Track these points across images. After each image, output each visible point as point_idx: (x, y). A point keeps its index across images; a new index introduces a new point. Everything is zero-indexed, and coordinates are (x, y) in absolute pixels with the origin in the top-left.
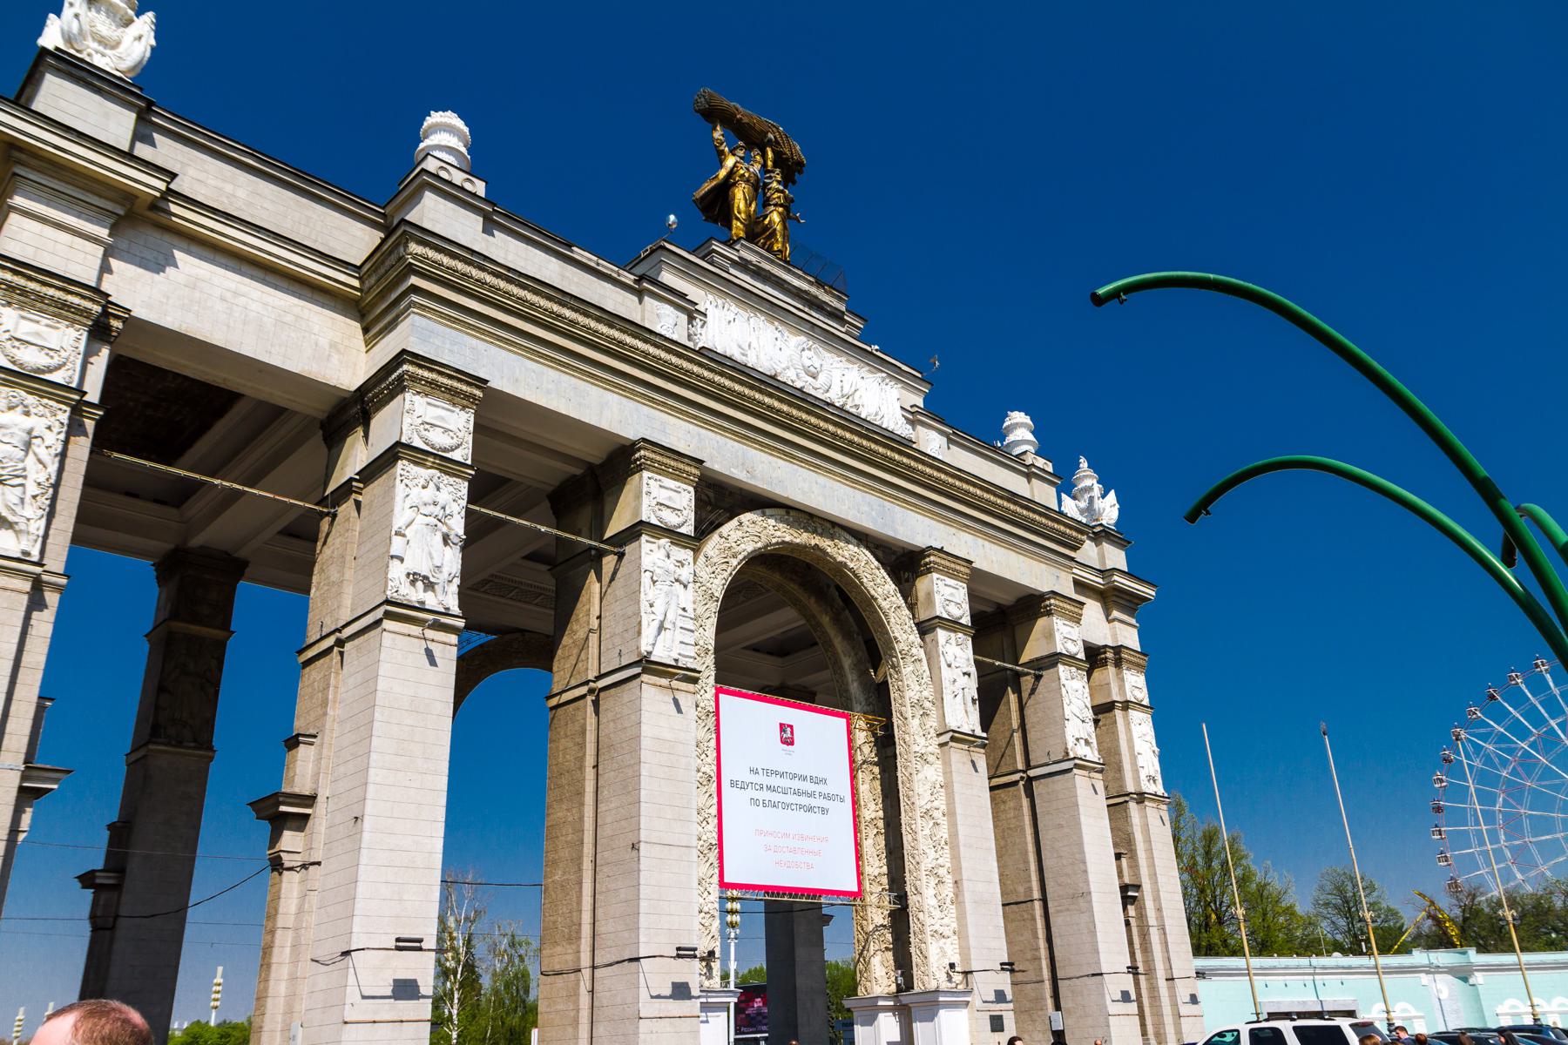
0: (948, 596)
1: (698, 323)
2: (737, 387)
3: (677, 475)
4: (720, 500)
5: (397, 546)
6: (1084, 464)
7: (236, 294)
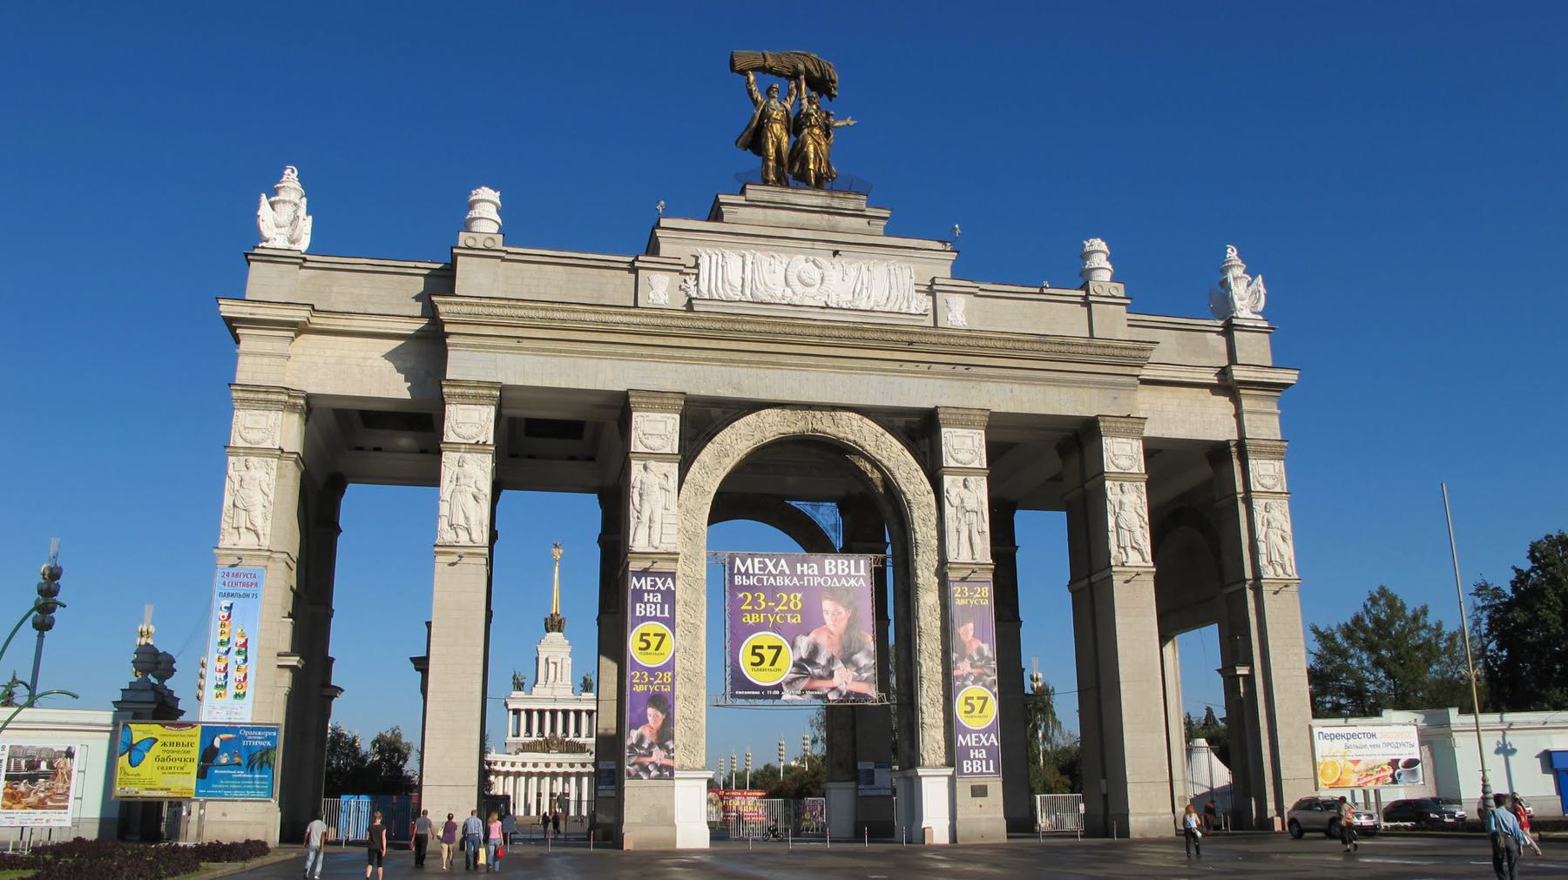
0: (964, 447)
2: (718, 325)
3: (664, 408)
6: (1232, 253)
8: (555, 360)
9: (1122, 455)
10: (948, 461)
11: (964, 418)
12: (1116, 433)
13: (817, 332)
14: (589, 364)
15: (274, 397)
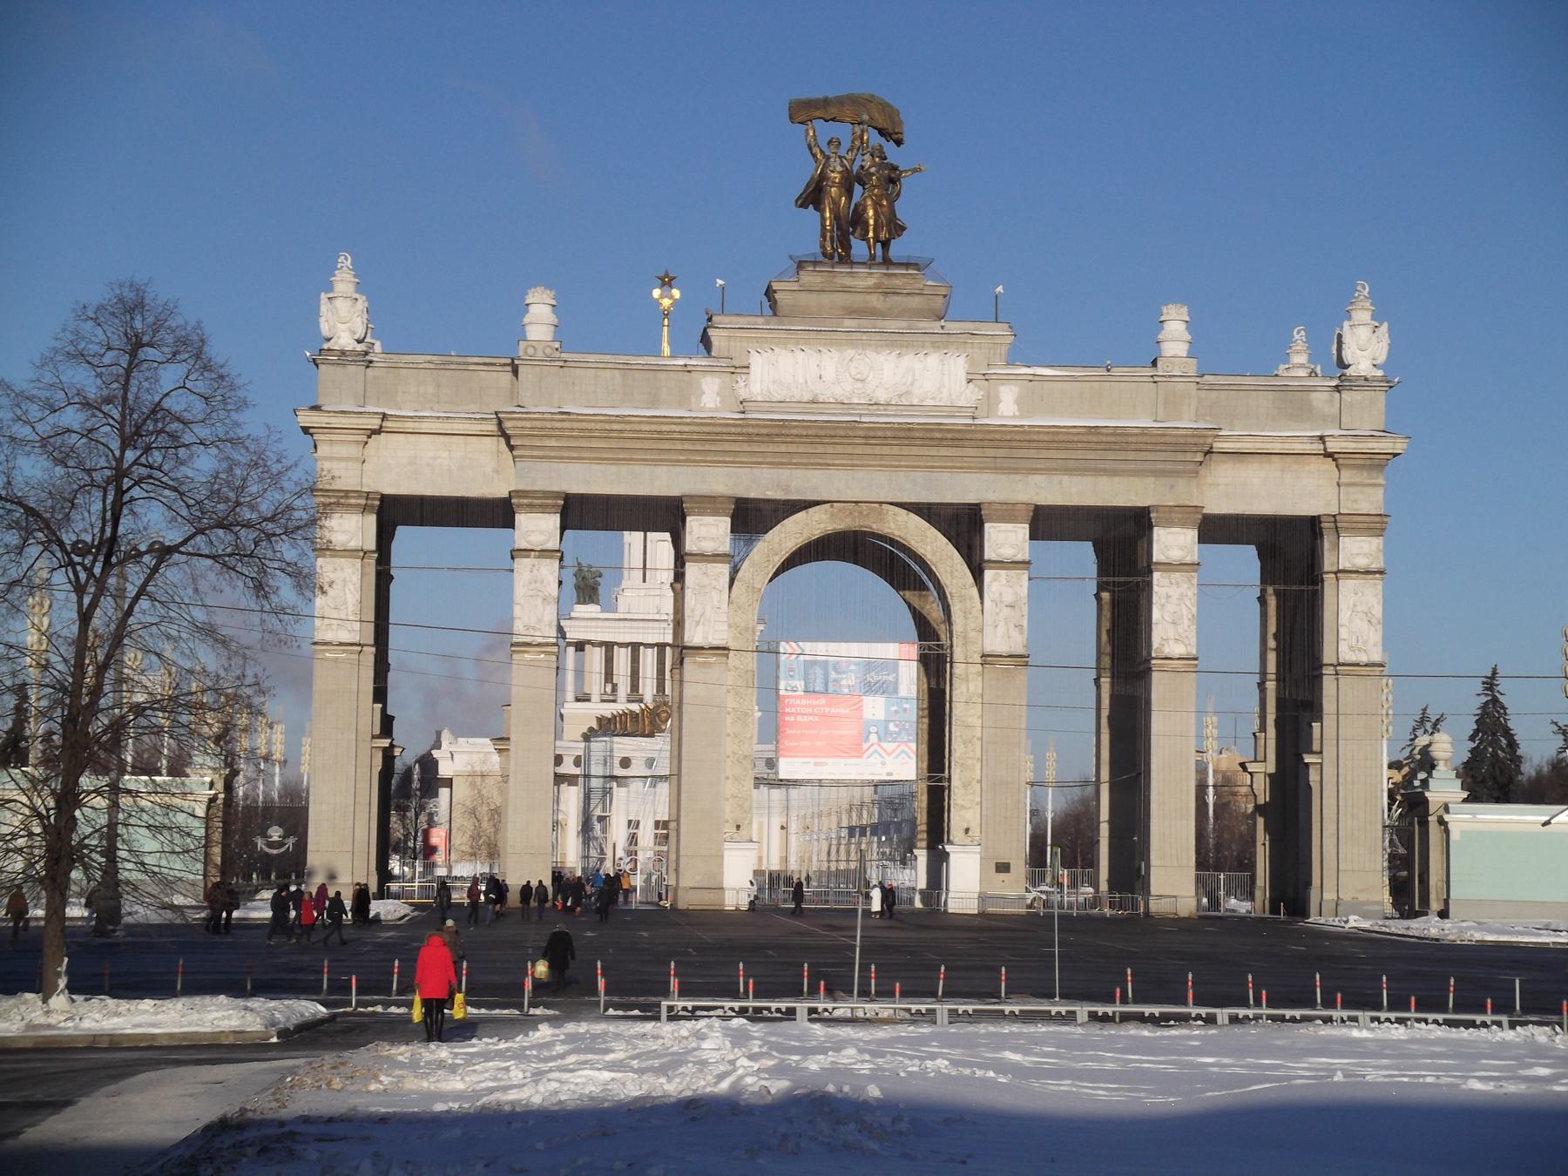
1: (741, 380)
2: (765, 431)
3: (715, 513)
4: (751, 518)
5: (517, 611)
7: (435, 458)
8: (614, 468)
9: (1172, 543)
10: (989, 554)
11: (1008, 513)
12: (1169, 523)
13: (862, 433)
14: (645, 471)
15: (353, 501)
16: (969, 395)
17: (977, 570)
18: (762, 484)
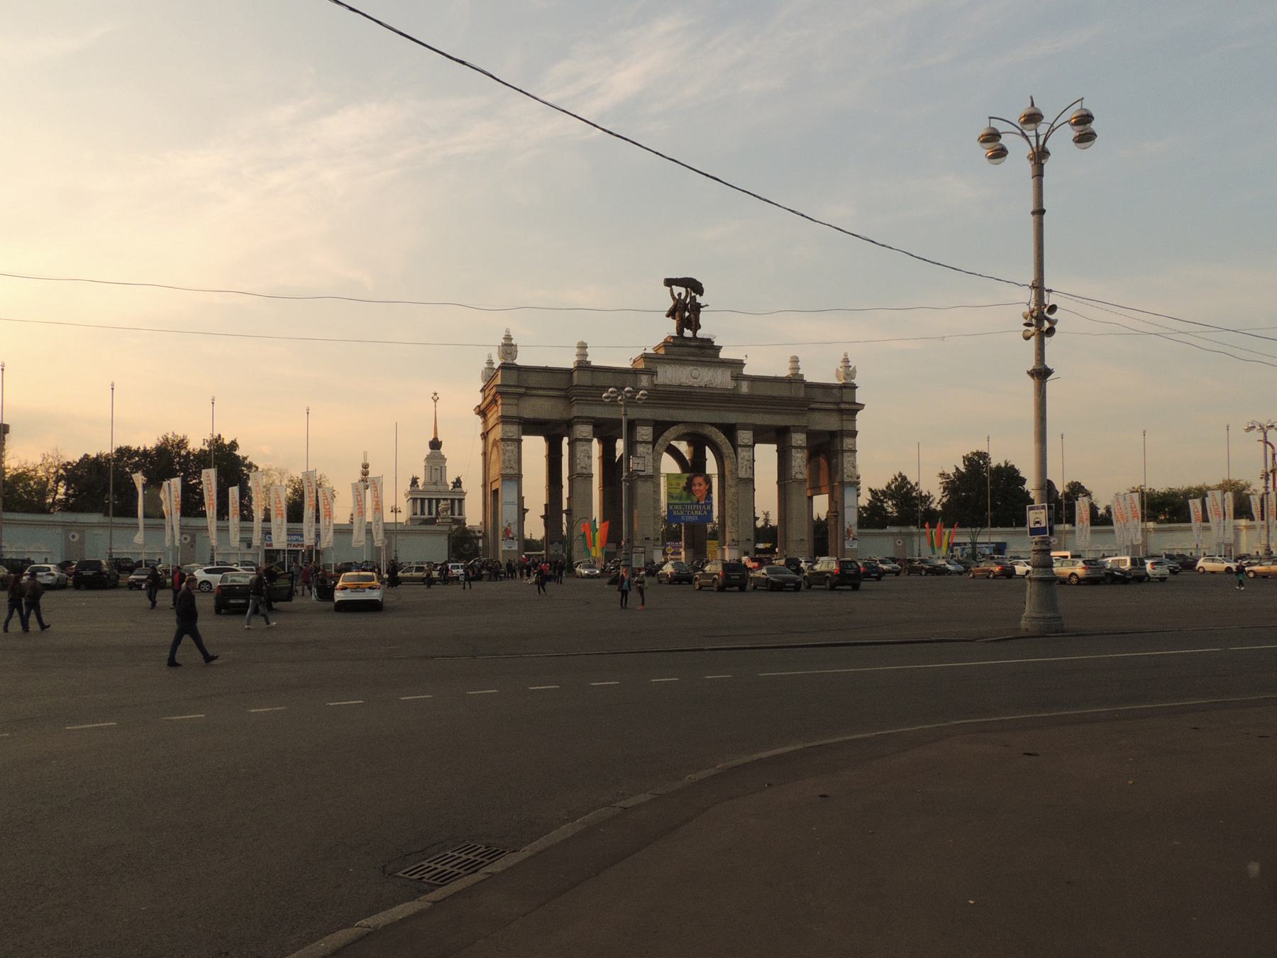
9: (799, 439)
10: (740, 442)
11: (745, 427)
12: (796, 432)
16: (730, 384)
17: (735, 446)
18: (663, 414)
